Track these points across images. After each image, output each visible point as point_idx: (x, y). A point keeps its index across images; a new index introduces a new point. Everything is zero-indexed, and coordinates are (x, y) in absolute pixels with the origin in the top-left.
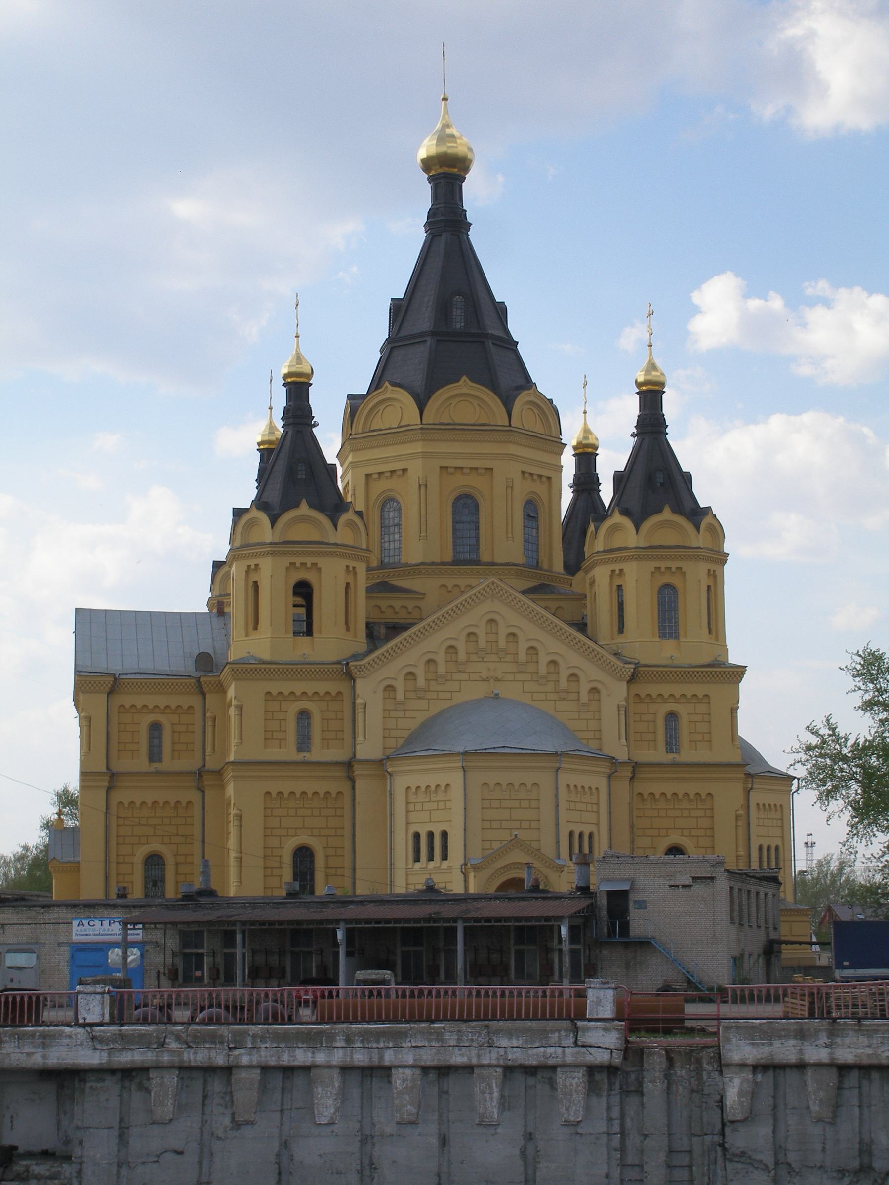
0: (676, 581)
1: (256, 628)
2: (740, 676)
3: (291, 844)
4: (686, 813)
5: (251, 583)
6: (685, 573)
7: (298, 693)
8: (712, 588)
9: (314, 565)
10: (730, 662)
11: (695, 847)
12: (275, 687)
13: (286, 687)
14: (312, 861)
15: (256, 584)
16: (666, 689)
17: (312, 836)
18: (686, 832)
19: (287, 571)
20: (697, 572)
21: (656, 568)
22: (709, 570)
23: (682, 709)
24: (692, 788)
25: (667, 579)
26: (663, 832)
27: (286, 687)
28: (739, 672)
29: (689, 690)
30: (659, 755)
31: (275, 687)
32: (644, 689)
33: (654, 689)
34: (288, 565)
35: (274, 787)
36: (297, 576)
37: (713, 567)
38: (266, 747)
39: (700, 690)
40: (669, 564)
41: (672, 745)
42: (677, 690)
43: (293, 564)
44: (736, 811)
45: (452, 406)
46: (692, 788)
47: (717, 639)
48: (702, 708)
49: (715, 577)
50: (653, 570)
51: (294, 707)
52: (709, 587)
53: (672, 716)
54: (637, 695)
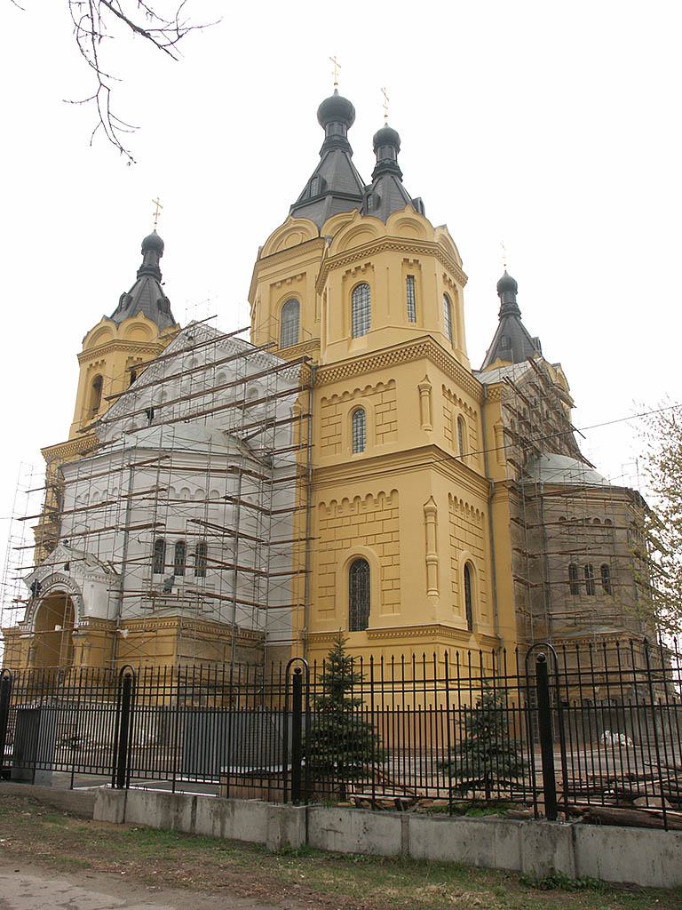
16: (350, 386)
21: (347, 272)
22: (406, 260)
23: (368, 403)
25: (360, 278)
29: (372, 380)
30: (346, 455)
32: (327, 392)
33: (338, 389)
39: (384, 377)
41: (358, 444)
42: (360, 383)
43: (91, 365)
46: (373, 487)
48: (388, 396)
53: (358, 413)
54: (325, 398)
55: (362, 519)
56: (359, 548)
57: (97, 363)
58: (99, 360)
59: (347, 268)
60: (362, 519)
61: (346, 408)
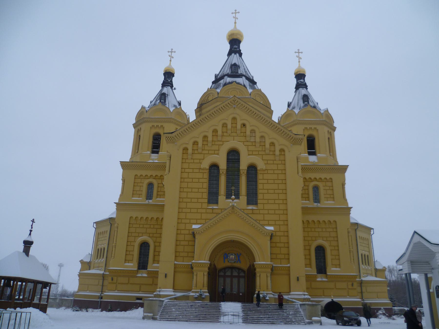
0: (314, 133)
1: (137, 152)
2: (345, 170)
3: (140, 240)
4: (324, 230)
5: (138, 136)
6: (318, 130)
7: (149, 176)
8: (330, 138)
9: (162, 126)
10: (340, 164)
11: (329, 246)
12: (139, 173)
13: (144, 173)
14: (149, 249)
15: (140, 136)
17: (149, 237)
18: (325, 239)
19: (151, 129)
20: (323, 130)
22: (328, 131)
23: (320, 184)
24: (327, 218)
26: (314, 239)
27: (144, 173)
28: (344, 168)
31: (139, 173)
34: (151, 126)
35: (135, 214)
36: (154, 131)
37: (330, 130)
38: (132, 197)
40: (311, 126)
41: (317, 199)
43: (153, 126)
44: (348, 229)
45: (230, 92)
47: (333, 157)
48: (329, 184)
49: (331, 134)
50: (304, 128)
51: (146, 182)
52: (329, 138)
55: (320, 230)
56: (320, 242)
57: (157, 126)
58: (160, 125)
59: (306, 126)
60: (320, 230)
61: (312, 184)
